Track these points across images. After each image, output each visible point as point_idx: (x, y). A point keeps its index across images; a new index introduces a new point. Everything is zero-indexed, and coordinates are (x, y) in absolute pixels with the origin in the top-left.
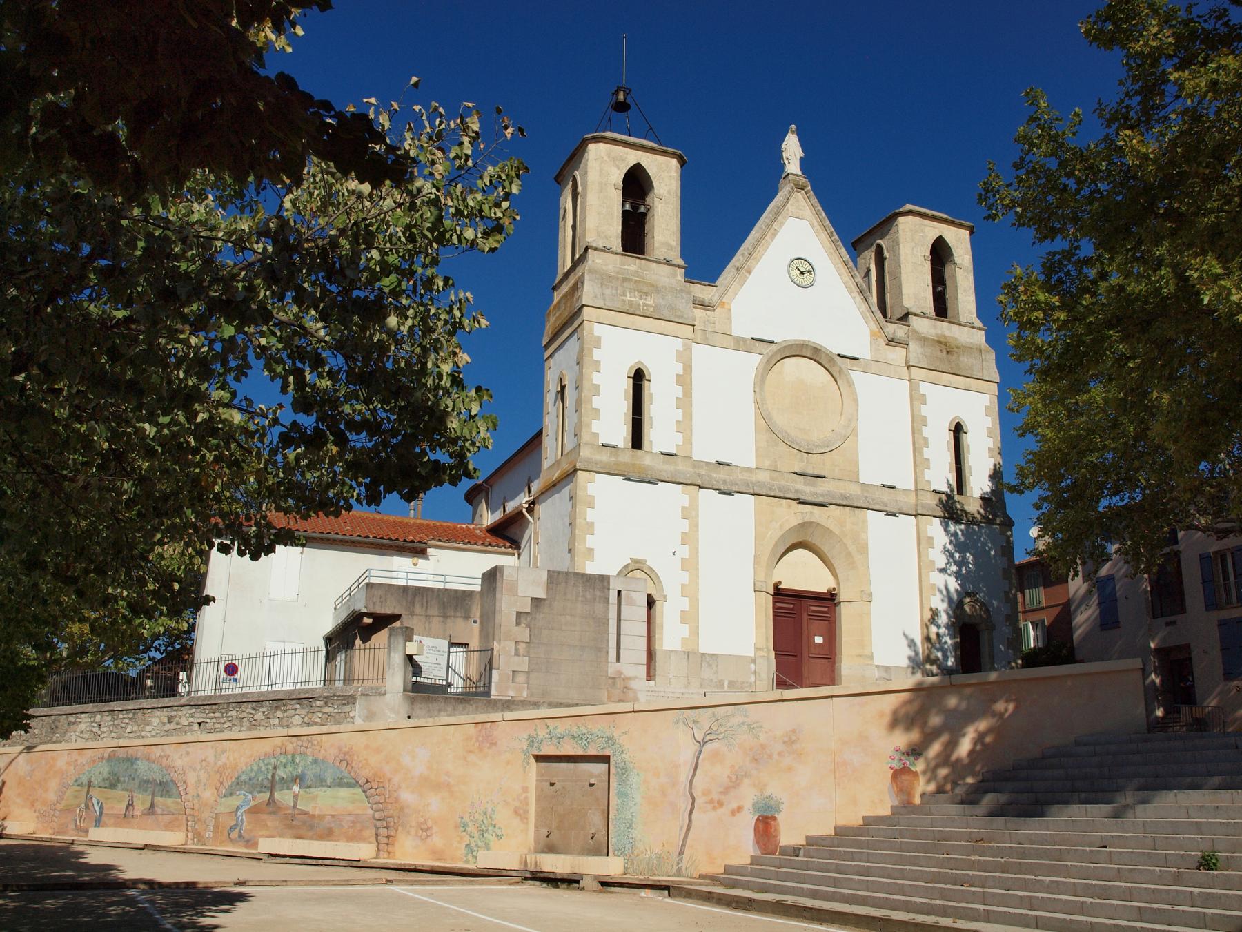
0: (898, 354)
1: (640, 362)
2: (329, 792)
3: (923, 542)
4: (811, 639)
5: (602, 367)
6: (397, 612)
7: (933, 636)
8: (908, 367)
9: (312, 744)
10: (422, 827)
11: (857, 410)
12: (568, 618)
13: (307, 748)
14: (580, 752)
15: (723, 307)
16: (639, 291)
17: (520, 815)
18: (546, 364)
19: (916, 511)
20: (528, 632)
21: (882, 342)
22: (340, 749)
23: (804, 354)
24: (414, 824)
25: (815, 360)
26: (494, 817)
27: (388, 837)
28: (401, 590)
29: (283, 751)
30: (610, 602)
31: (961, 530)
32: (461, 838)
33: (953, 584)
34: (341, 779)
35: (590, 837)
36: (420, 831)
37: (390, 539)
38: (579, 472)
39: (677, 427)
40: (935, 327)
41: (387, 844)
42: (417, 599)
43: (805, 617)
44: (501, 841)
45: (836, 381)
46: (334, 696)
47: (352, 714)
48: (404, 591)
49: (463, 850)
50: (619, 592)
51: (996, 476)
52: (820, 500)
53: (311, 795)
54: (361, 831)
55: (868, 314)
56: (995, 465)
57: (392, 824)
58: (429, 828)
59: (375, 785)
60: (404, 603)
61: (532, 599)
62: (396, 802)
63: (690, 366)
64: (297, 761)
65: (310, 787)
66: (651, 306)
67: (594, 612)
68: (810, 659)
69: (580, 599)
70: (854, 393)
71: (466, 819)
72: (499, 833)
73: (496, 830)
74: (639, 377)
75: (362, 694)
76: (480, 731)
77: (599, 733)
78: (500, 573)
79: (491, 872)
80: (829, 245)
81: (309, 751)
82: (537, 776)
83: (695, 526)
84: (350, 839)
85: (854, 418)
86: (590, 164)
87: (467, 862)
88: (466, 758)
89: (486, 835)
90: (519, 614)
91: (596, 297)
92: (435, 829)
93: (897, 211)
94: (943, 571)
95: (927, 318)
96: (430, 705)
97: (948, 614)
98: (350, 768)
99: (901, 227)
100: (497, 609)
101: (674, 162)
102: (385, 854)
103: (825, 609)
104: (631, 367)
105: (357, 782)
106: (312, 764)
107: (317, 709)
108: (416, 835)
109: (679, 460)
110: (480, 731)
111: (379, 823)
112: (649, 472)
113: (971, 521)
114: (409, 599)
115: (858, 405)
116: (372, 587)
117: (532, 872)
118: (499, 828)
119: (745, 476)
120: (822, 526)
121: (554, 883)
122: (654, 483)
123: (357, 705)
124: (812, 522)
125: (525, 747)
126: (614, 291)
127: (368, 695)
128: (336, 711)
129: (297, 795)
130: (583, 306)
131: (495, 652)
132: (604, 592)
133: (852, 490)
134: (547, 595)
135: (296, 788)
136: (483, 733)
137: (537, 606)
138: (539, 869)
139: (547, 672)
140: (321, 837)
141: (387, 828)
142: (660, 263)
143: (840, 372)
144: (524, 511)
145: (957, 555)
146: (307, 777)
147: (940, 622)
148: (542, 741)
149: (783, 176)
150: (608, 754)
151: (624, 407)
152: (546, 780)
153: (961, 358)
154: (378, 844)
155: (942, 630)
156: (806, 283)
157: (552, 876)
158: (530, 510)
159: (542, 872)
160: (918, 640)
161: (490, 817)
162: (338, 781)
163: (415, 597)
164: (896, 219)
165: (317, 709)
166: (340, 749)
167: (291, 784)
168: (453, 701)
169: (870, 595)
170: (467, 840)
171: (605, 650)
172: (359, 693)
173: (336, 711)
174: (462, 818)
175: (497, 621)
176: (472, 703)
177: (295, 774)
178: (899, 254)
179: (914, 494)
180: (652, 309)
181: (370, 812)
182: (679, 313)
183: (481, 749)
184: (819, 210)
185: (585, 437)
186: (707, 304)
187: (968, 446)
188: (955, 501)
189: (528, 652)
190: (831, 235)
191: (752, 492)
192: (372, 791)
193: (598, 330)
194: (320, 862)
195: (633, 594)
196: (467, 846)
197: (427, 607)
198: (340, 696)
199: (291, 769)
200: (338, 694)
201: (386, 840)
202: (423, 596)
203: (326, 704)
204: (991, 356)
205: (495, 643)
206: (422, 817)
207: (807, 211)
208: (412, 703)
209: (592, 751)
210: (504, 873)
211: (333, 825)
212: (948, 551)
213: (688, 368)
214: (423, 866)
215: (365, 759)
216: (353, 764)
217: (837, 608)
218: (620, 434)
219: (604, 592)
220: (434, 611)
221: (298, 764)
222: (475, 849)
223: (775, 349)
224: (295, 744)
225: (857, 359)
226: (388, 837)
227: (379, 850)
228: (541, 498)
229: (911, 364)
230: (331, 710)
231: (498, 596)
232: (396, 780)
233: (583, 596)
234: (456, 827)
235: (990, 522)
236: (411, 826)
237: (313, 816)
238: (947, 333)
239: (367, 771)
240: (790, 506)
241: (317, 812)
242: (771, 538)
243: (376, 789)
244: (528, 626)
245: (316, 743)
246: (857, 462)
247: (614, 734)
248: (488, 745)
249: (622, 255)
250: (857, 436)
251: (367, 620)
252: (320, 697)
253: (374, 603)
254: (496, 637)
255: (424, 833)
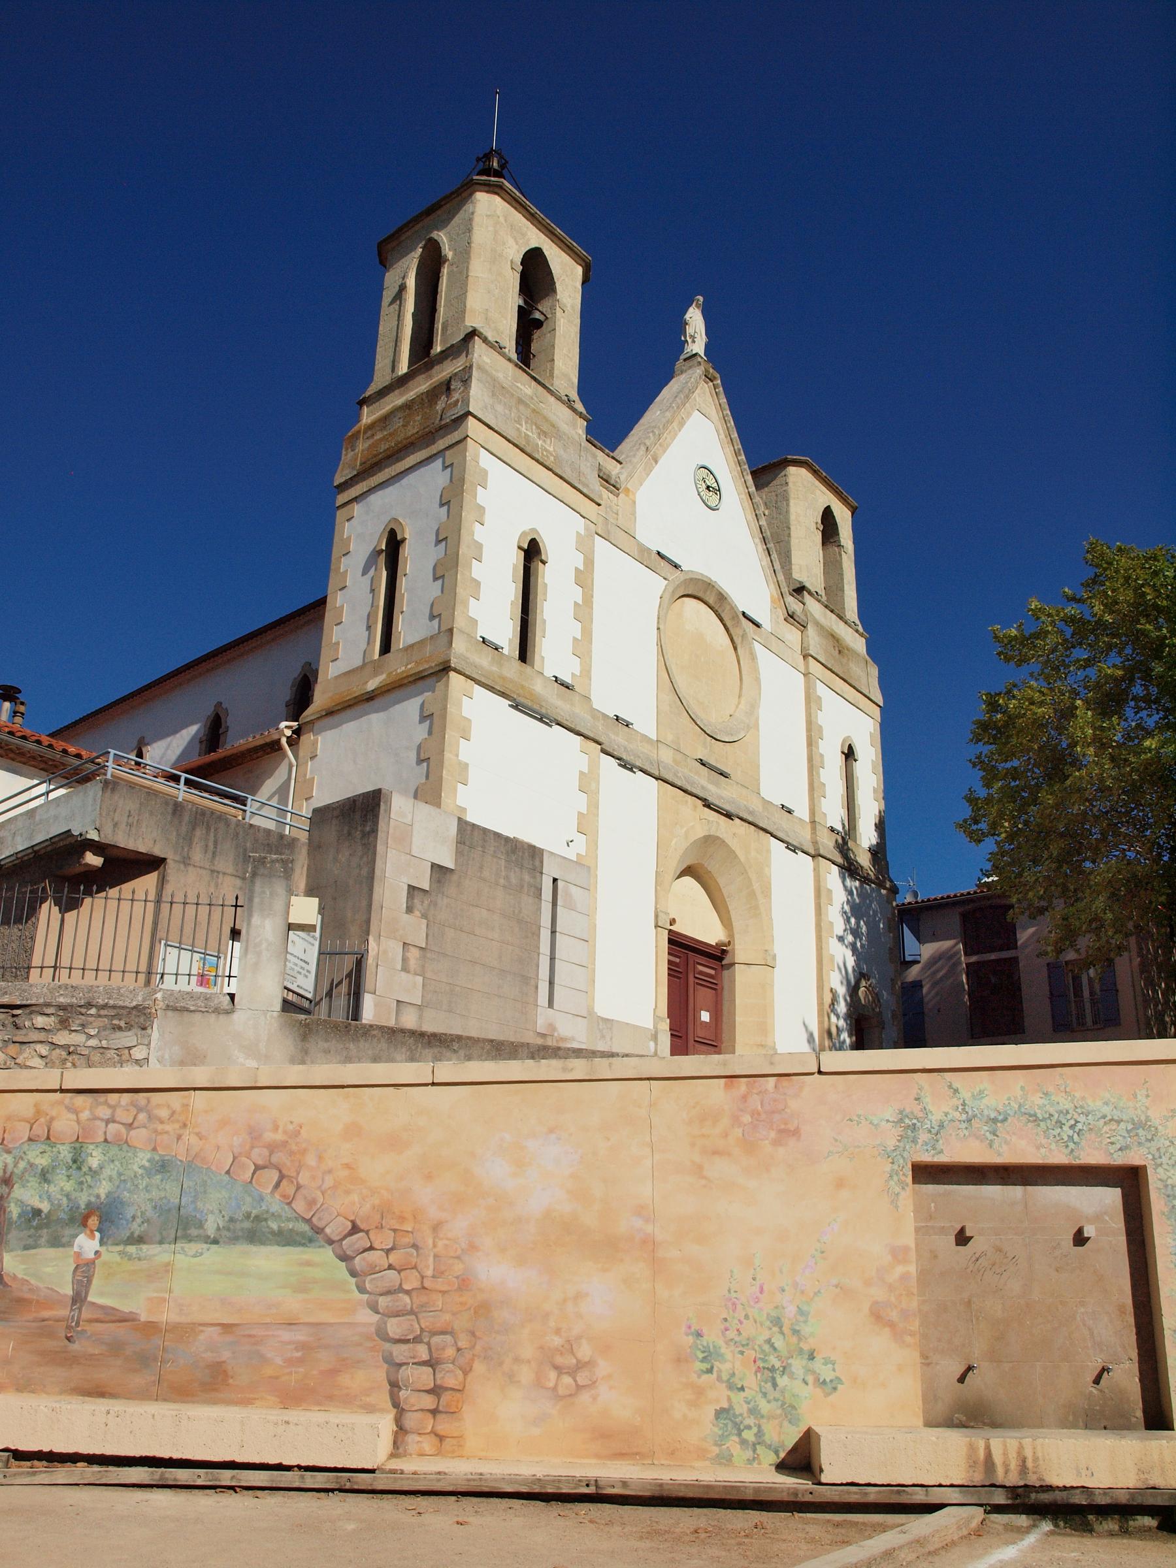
0: (792, 635)
1: (534, 530)
2: (213, 1256)
3: (820, 894)
4: (696, 1017)
5: (487, 519)
6: (158, 851)
7: (834, 1030)
8: (805, 657)
9: (150, 1117)
10: (559, 1360)
11: (760, 694)
12: (484, 913)
13: (130, 1126)
14: (1059, 1157)
15: (627, 495)
16: (536, 424)
17: (891, 1325)
18: (339, 513)
19: (817, 849)
20: (424, 927)
21: (781, 614)
22: (254, 1134)
23: (707, 599)
24: (528, 1351)
25: (716, 612)
26: (806, 1330)
27: (436, 1391)
28: (170, 809)
29: (40, 1130)
30: (543, 897)
31: (856, 888)
32: (700, 1392)
33: (851, 962)
34: (258, 1218)
35: (1090, 1378)
36: (553, 1375)
37: (39, 742)
38: (452, 674)
39: (574, 648)
40: (825, 616)
41: (434, 1412)
42: (199, 833)
43: (691, 979)
44: (833, 1397)
45: (735, 649)
46: (89, 1005)
47: (138, 1053)
48: (174, 812)
49: (705, 1426)
50: (555, 880)
51: (880, 827)
52: (728, 807)
53: (144, 1264)
54: (333, 1372)
55: (769, 572)
56: (880, 812)
57: (450, 1352)
58: (580, 1366)
59: (383, 1240)
60: (173, 837)
61: (433, 865)
62: (461, 1289)
63: (592, 563)
64: (94, 1162)
65: (140, 1240)
66: (552, 455)
67: (520, 912)
68: (697, 1045)
69: (502, 881)
70: (755, 670)
71: (713, 1337)
72: (827, 1374)
73: (817, 1365)
74: (532, 552)
75: (168, 1007)
76: (744, 1098)
77: (1106, 1110)
78: (386, 802)
79: (872, 1496)
80: (734, 466)
81: (139, 1136)
82: (916, 1221)
83: (594, 805)
84: (292, 1398)
85: (754, 706)
86: (477, 220)
87: (725, 1460)
88: (700, 1168)
89: (782, 1381)
90: (412, 889)
91: (486, 407)
92: (603, 1367)
93: (789, 457)
94: (841, 939)
95: (819, 601)
96: (352, 1046)
97: (846, 1000)
98: (291, 1190)
99: (791, 480)
100: (378, 872)
101: (579, 270)
102: (428, 1444)
103: (712, 972)
104: (524, 534)
105: (319, 1231)
106: (149, 1173)
107: (35, 1036)
108: (539, 1383)
109: (577, 698)
110: (744, 1098)
111: (400, 1352)
112: (543, 704)
113: (865, 880)
114: (184, 829)
115: (760, 689)
116: (113, 790)
117: (1012, 1490)
118: (827, 1361)
119: (645, 749)
120: (727, 846)
121: (1077, 1518)
122: (546, 724)
123: (155, 1034)
124: (718, 838)
125: (891, 1143)
126: (507, 412)
127: (188, 1010)
128: (93, 1042)
129: (91, 1264)
130: (469, 413)
131: (370, 961)
132: (535, 877)
133: (756, 805)
134: (456, 864)
135: (87, 1244)
136: (755, 1102)
137: (439, 882)
138: (1032, 1480)
139: (450, 1011)
140: (181, 1393)
141: (432, 1363)
142: (559, 399)
143: (743, 636)
144: (284, 741)
145: (853, 920)
146: (130, 1212)
147: (839, 1011)
148: (941, 1126)
149: (682, 357)
150: (1137, 1162)
151: (512, 592)
152: (942, 1231)
153: (851, 665)
154: (400, 1411)
155: (842, 1023)
156: (713, 505)
157: (1079, 1499)
158: (292, 742)
159: (1050, 1488)
160: (815, 1029)
161: (796, 1332)
162: (247, 1225)
163: (194, 829)
164: (785, 467)
165: (35, 1036)
166: (254, 1134)
167: (68, 1232)
168: (411, 1041)
169: (774, 957)
170: (720, 1396)
171: (533, 982)
172: (161, 1005)
173: (93, 1042)
174: (699, 1335)
175: (376, 897)
176: (456, 1046)
177: (83, 1199)
178: (788, 512)
179: (808, 828)
180: (552, 458)
181: (367, 1318)
182: (583, 479)
183: (749, 1146)
184: (727, 414)
185: (459, 623)
186: (612, 482)
187: (857, 778)
188: (849, 849)
189: (423, 966)
190: (737, 454)
191: (657, 773)
192: (371, 1256)
193: (486, 460)
194: (226, 1477)
195: (574, 890)
196: (719, 1413)
197: (214, 853)
198: (105, 1006)
199: (68, 1186)
200: (101, 1002)
201: (428, 1402)
202: (208, 828)
203: (64, 1024)
204: (874, 671)
205: (371, 939)
206: (558, 1331)
207: (713, 411)
208: (304, 1038)
209: (1092, 1155)
210: (919, 1497)
211: (226, 1355)
212: (845, 913)
213: (589, 562)
214: (624, 1484)
215: (347, 1166)
216: (303, 1178)
217: (726, 973)
218: (506, 634)
219: (535, 877)
220: (226, 863)
221: (94, 1173)
222: (750, 1421)
223: (682, 579)
224: (85, 1115)
225: (758, 625)
226: (436, 1391)
227: (401, 1430)
228: (317, 725)
229: (811, 652)
230: (78, 1039)
231: (380, 848)
232: (459, 1226)
233: (507, 878)
234: (680, 1360)
235: (881, 885)
236: (517, 1360)
237: (151, 1328)
238: (834, 627)
239: (355, 1197)
240: (695, 807)
241: (166, 1316)
242: (676, 849)
243: (388, 1252)
244: (424, 916)
245: (164, 1113)
246: (757, 767)
247: (1149, 1113)
248: (773, 1134)
249: (516, 365)
250: (758, 730)
251: (93, 860)
252: (48, 1005)
253: (116, 825)
254: (373, 928)
255: (567, 1380)
